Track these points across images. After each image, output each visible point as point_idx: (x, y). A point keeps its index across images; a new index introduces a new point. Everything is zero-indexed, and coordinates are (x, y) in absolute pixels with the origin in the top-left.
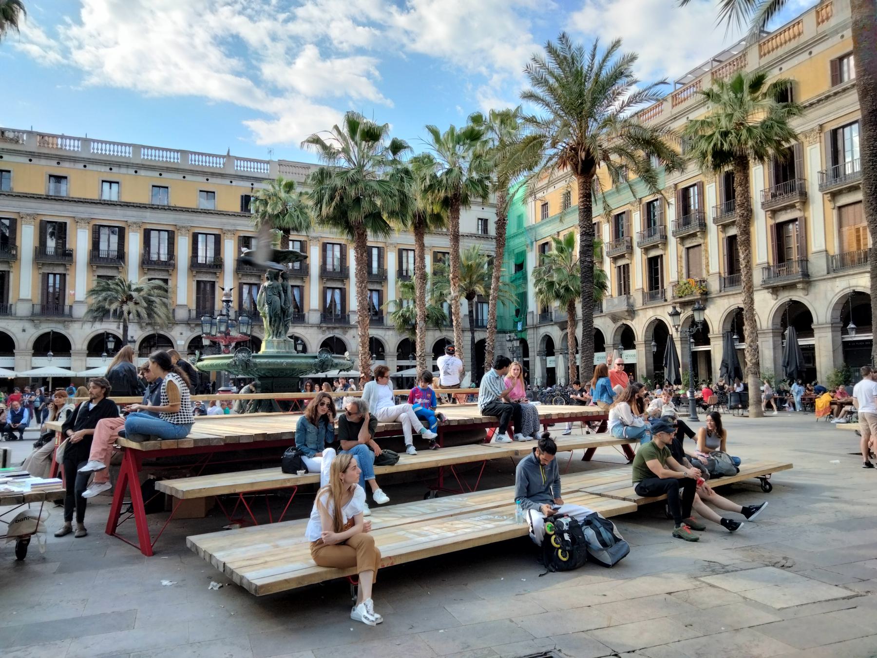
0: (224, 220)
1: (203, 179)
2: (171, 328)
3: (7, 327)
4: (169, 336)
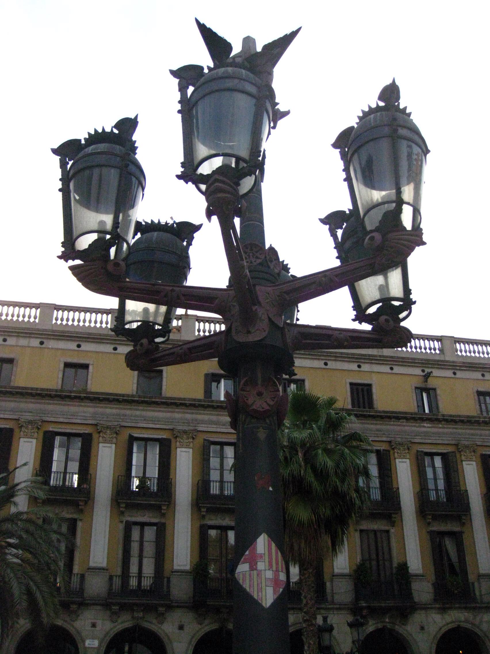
0: (178, 415)
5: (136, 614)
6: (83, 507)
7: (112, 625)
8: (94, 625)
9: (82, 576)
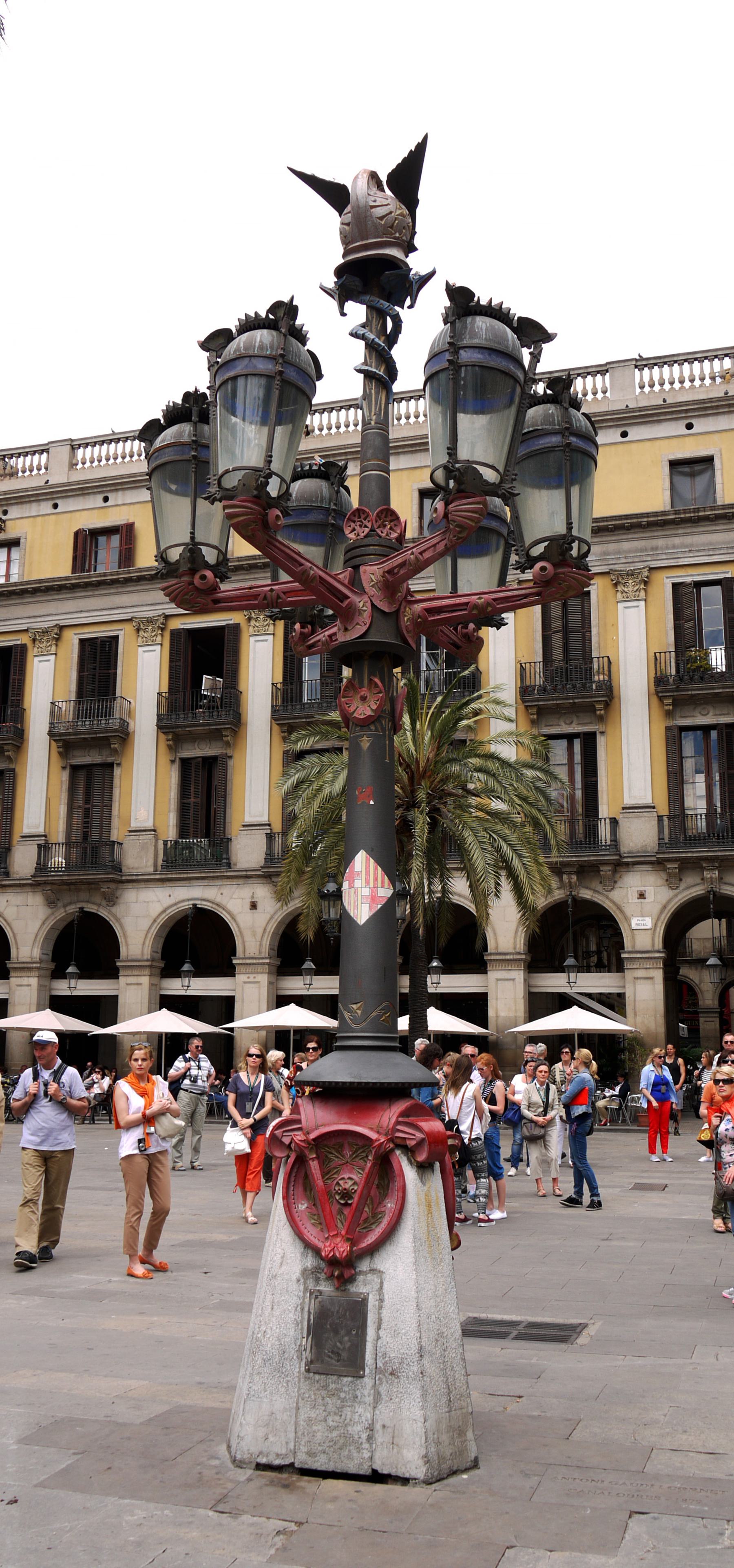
1: (679, 428)
2: (612, 883)
3: (219, 899)
4: (607, 905)
5: (707, 875)
6: (602, 712)
7: (671, 893)
8: (642, 896)
9: (614, 822)
